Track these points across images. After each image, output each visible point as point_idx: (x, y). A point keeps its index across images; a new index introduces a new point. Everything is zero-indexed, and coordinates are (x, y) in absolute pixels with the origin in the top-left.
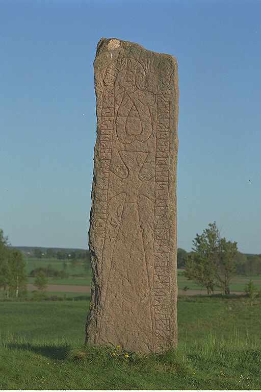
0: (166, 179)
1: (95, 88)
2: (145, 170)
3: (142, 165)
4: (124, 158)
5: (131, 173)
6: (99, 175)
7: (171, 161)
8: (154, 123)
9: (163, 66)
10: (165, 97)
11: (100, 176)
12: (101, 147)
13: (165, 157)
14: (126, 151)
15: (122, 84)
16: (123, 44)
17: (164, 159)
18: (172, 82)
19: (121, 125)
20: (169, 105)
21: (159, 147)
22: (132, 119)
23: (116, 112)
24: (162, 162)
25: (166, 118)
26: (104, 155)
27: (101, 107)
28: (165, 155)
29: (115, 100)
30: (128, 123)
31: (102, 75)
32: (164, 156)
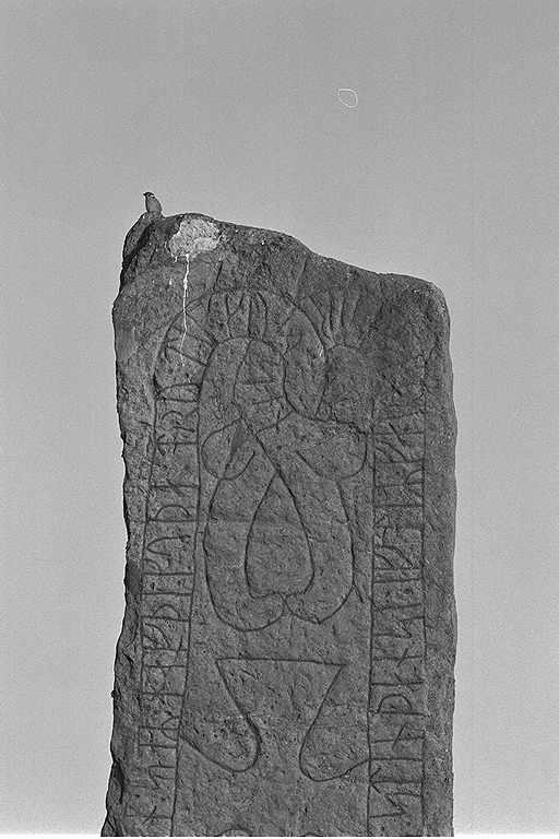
0: (412, 770)
1: (119, 411)
2: (327, 735)
3: (311, 714)
4: (239, 685)
5: (270, 745)
6: (135, 759)
7: (432, 698)
8: (362, 546)
9: (401, 319)
10: (403, 443)
11: (143, 759)
12: (147, 643)
13: (409, 684)
14: (248, 657)
15: (228, 395)
16: (232, 234)
17: (404, 689)
18: (431, 383)
19: (229, 555)
20: (419, 475)
21: (385, 640)
22: (272, 530)
23: (206, 501)
24: (397, 700)
25: (409, 525)
26: (157, 674)
27: (145, 484)
28: (407, 674)
29: (202, 453)
30: (256, 547)
31: (149, 356)
32: (404, 676)
